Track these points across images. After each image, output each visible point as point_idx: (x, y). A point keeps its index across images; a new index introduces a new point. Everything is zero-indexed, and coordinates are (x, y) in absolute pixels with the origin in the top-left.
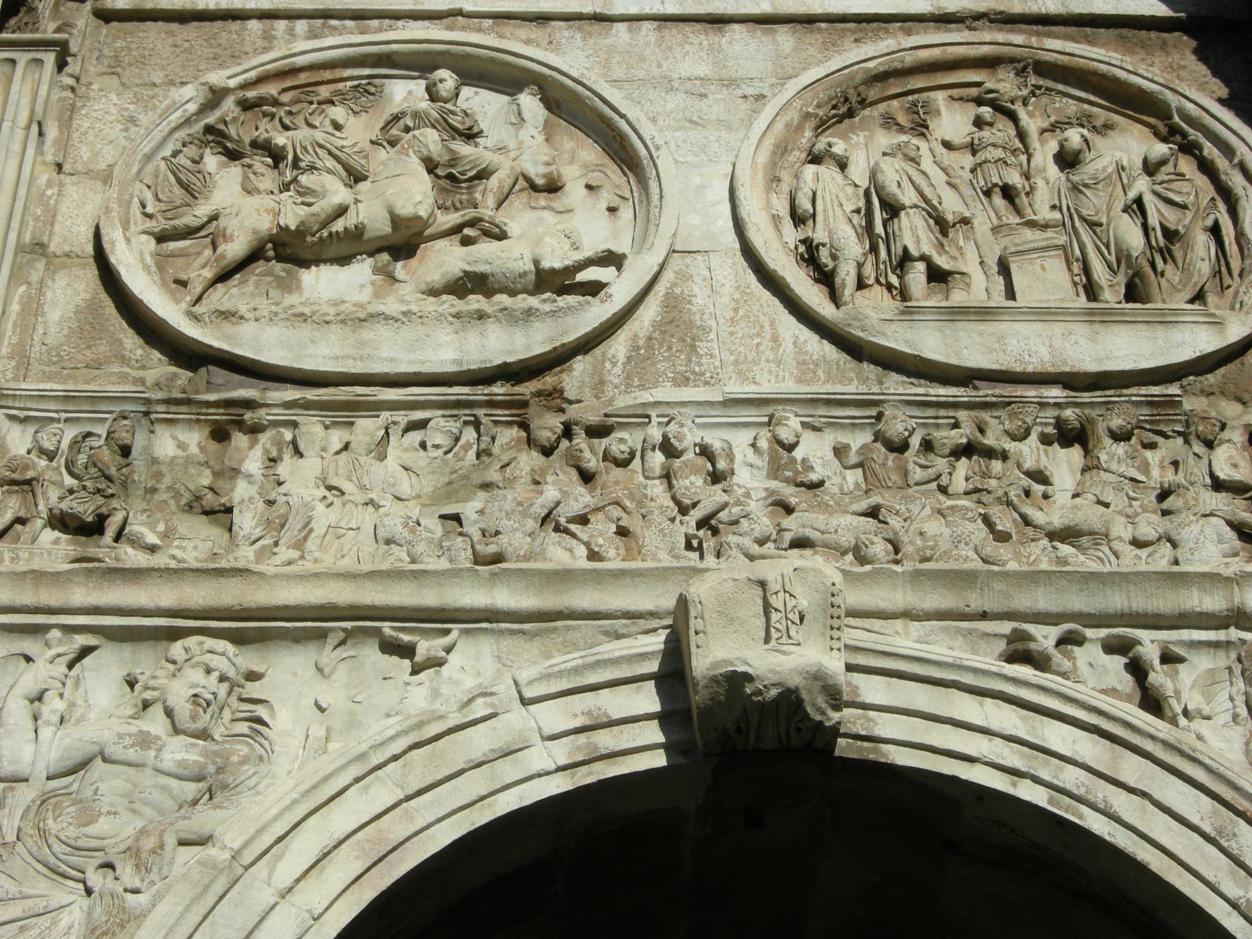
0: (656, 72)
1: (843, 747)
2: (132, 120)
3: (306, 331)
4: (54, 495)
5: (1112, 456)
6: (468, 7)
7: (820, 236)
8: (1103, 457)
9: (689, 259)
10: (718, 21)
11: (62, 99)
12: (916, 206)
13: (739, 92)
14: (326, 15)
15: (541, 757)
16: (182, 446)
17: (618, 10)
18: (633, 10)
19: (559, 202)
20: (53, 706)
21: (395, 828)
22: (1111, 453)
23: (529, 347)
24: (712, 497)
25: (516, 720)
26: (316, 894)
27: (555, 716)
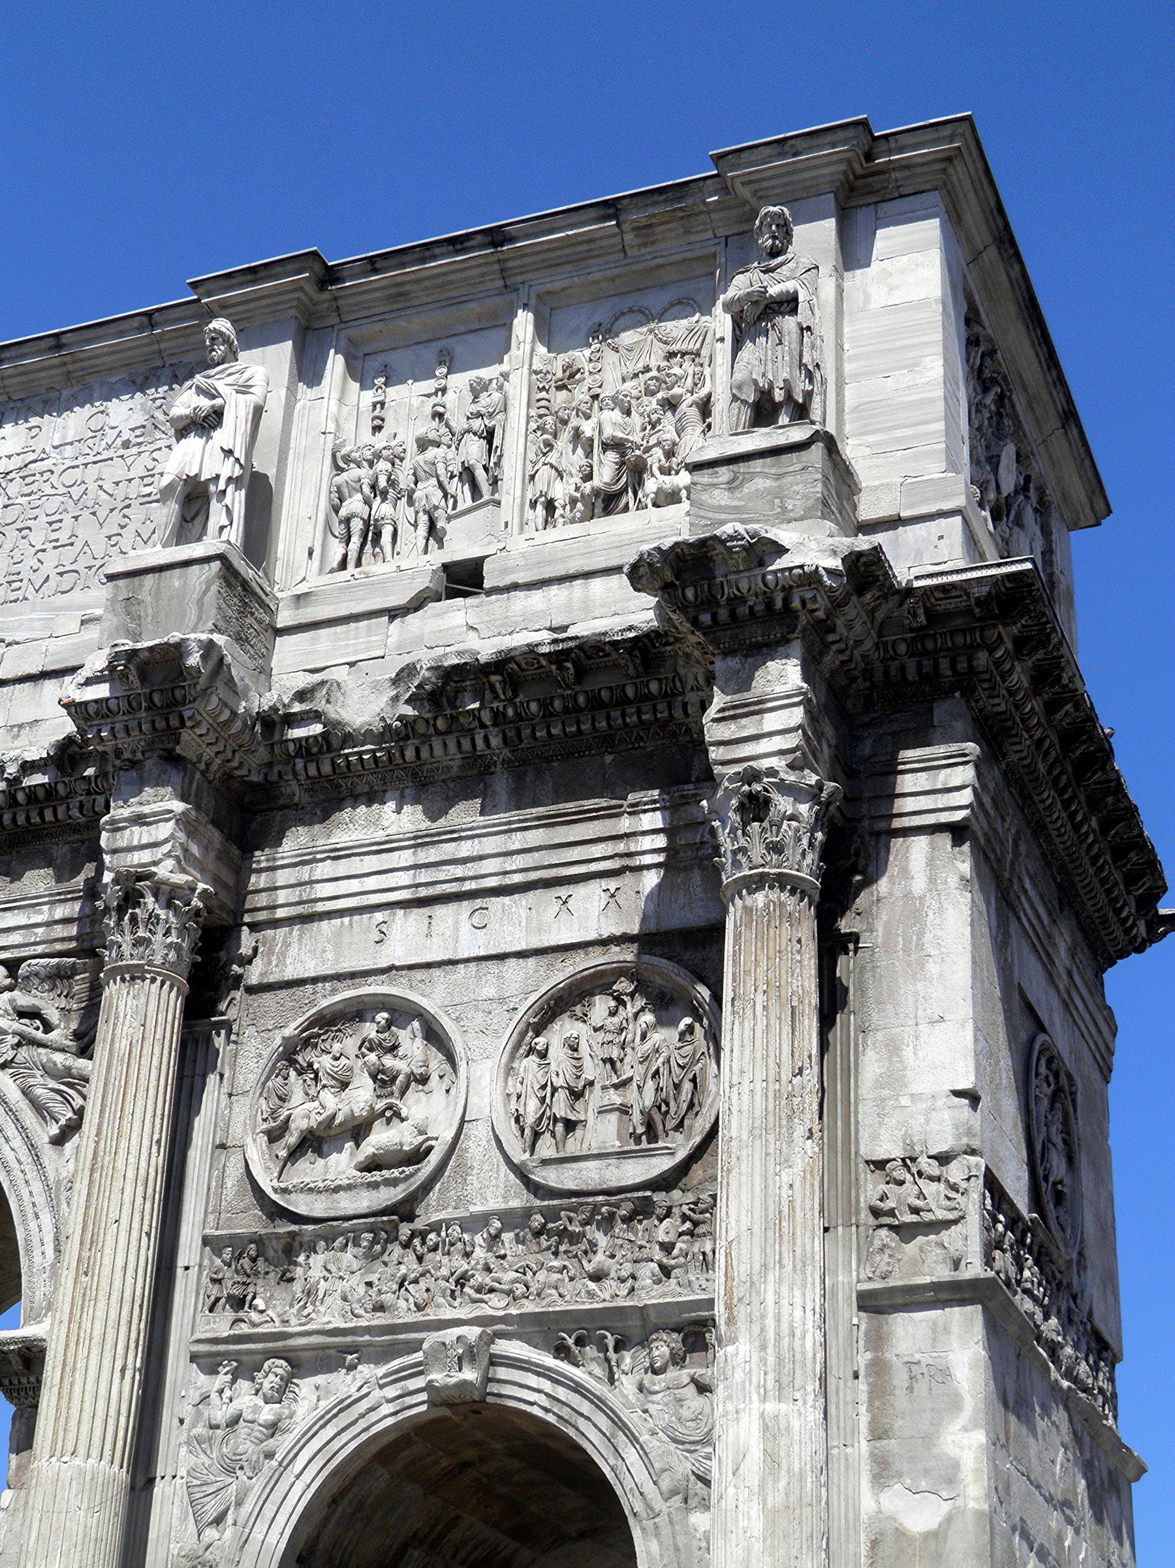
0: (473, 996)
1: (490, 1399)
2: (260, 1055)
3: (313, 1196)
4: (230, 1283)
5: (621, 1229)
6: (397, 964)
7: (521, 1111)
8: (617, 1231)
9: (470, 1125)
10: (502, 957)
11: (231, 1051)
12: (562, 1087)
13: (505, 1007)
14: (338, 977)
15: (387, 1409)
16: (276, 1251)
17: (460, 956)
18: (466, 956)
19: (426, 1088)
20: (227, 1393)
21: (336, 1444)
22: (619, 1227)
23: (396, 1196)
24: (462, 1265)
25: (377, 1394)
26: (307, 1477)
27: (391, 1392)
